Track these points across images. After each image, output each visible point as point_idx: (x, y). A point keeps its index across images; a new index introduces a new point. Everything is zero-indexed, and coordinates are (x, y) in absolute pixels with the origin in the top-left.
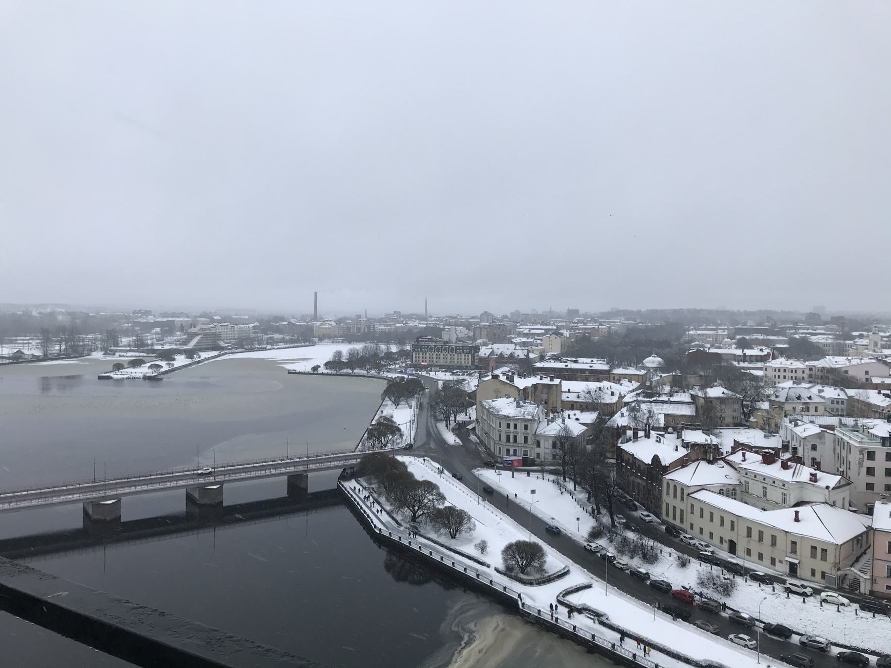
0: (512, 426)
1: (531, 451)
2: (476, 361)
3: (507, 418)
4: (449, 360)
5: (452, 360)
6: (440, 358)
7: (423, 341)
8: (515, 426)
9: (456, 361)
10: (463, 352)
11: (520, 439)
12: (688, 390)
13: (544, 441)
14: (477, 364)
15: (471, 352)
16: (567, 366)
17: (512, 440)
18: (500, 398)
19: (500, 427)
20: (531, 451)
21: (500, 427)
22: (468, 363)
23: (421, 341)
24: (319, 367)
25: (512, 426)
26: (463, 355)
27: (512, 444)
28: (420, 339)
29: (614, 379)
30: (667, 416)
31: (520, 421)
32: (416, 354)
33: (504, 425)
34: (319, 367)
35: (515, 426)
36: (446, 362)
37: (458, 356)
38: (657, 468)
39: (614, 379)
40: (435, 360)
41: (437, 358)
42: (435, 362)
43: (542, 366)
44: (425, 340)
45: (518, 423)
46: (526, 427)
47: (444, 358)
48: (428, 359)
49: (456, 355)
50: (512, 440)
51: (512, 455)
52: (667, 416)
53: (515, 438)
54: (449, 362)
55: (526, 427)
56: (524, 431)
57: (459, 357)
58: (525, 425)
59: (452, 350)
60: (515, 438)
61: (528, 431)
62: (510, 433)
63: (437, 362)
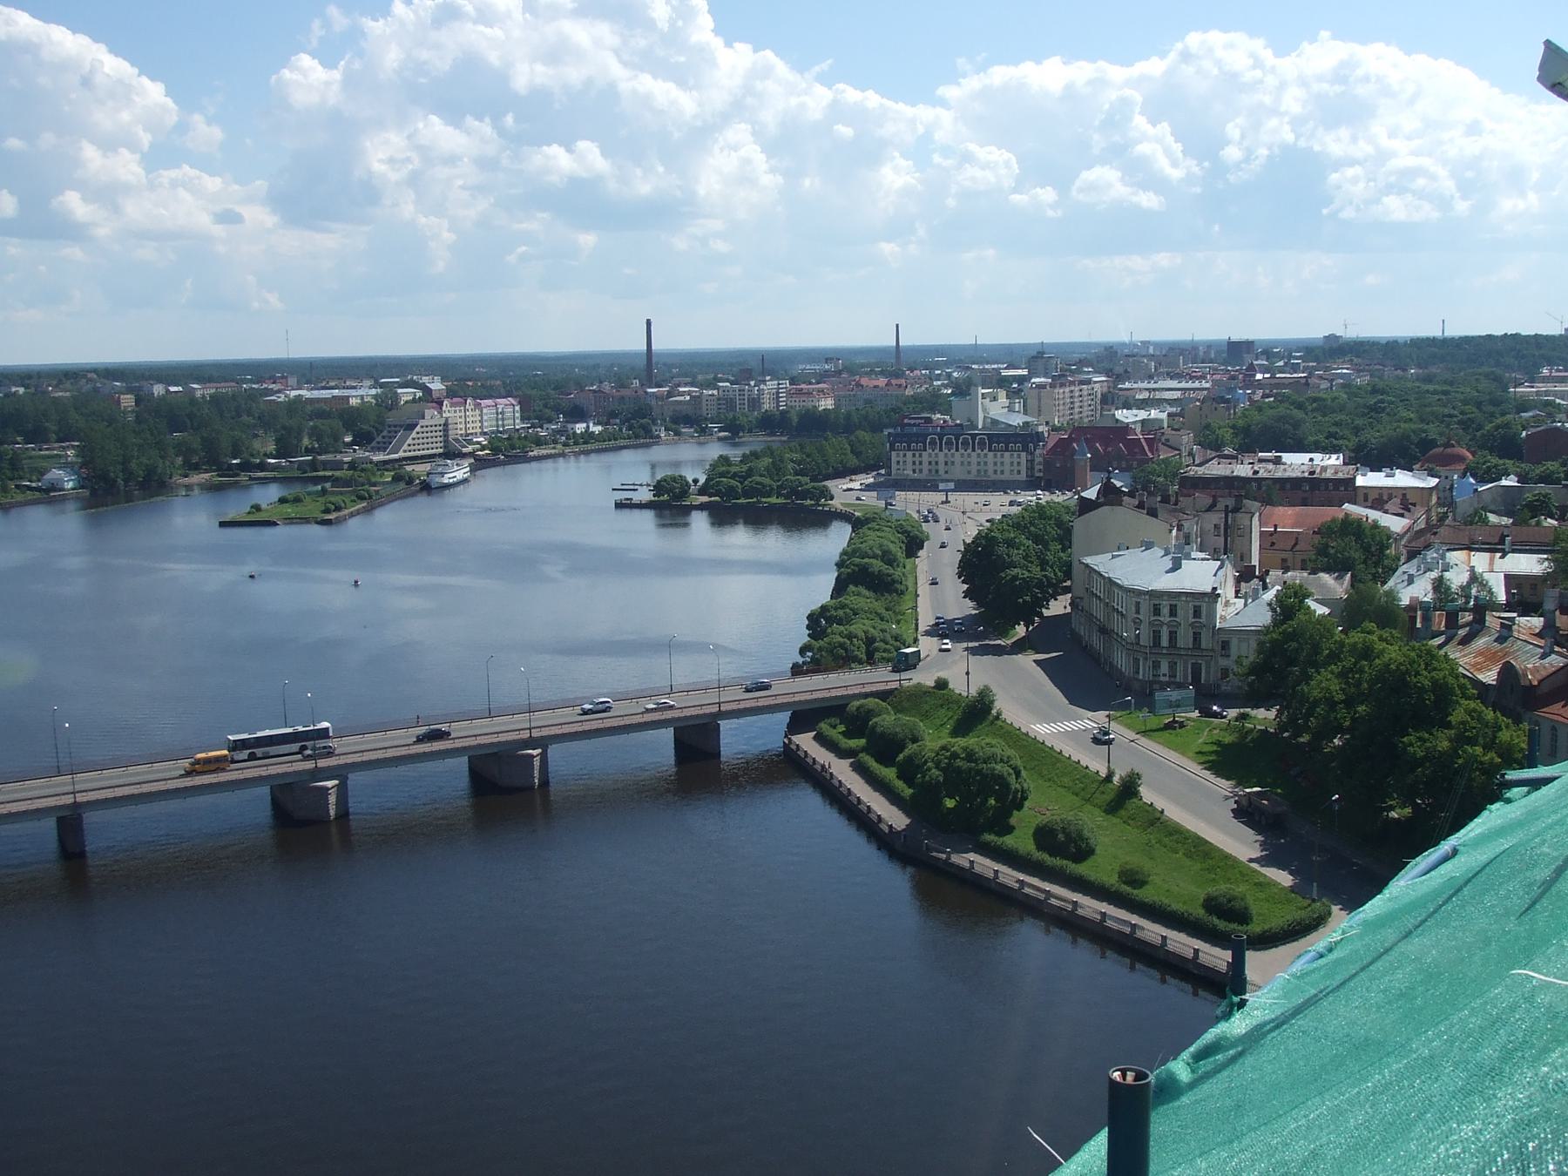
0: (1165, 611)
1: (1208, 667)
2: (1037, 467)
3: (1153, 594)
4: (974, 468)
5: (982, 467)
6: (953, 463)
7: (914, 425)
8: (1173, 612)
9: (991, 468)
10: (1007, 450)
11: (1186, 638)
12: (1545, 519)
13: (1240, 640)
14: (1041, 474)
15: (1025, 449)
16: (1256, 472)
17: (1165, 642)
18: (1128, 548)
19: (1138, 612)
20: (1208, 667)
21: (1138, 612)
22: (1019, 472)
23: (909, 425)
24: (1500, 558)
25: (1165, 611)
26: (1007, 454)
27: (1164, 652)
28: (906, 421)
29: (1366, 500)
30: (1510, 579)
31: (1184, 599)
32: (898, 455)
33: (1144, 608)
34: (1500, 558)
35: (1173, 612)
36: (969, 472)
37: (995, 456)
38: (1473, 689)
39: (1366, 500)
40: (941, 467)
41: (946, 463)
42: (941, 472)
43: (1228, 473)
44: (917, 421)
45: (1179, 604)
46: (1197, 612)
47: (962, 463)
48: (925, 467)
49: (991, 454)
50: (1165, 642)
51: (1164, 675)
52: (1510, 579)
53: (1173, 636)
54: (974, 472)
55: (1197, 612)
56: (1192, 620)
57: (999, 460)
58: (1195, 606)
59: (982, 444)
60: (1173, 636)
61: (1203, 620)
62: (1162, 623)
63: (946, 472)
